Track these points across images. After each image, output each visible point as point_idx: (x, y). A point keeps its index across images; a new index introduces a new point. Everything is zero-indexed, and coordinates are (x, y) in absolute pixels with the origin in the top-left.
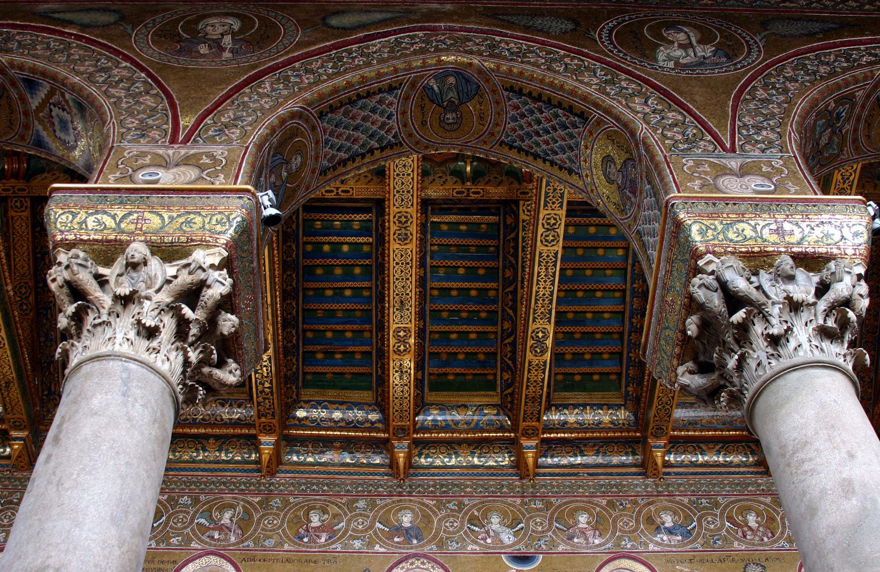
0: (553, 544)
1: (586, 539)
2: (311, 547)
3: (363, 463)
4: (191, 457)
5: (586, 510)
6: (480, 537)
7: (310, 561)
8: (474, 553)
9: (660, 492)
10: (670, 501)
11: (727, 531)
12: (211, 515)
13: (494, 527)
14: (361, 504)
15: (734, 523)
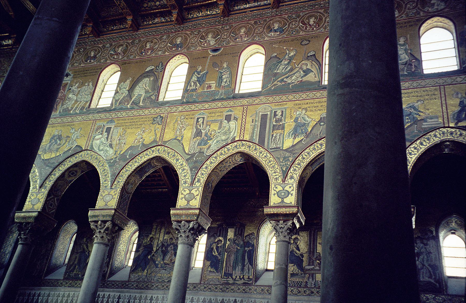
0: (229, 42)
1: (242, 39)
2: (145, 56)
3: (169, 21)
4: (112, 29)
5: (244, 27)
6: (203, 44)
7: (143, 61)
8: (199, 50)
9: (277, 14)
10: (280, 18)
11: (300, 28)
12: (115, 50)
13: (208, 39)
14: (165, 37)
15: (304, 24)
